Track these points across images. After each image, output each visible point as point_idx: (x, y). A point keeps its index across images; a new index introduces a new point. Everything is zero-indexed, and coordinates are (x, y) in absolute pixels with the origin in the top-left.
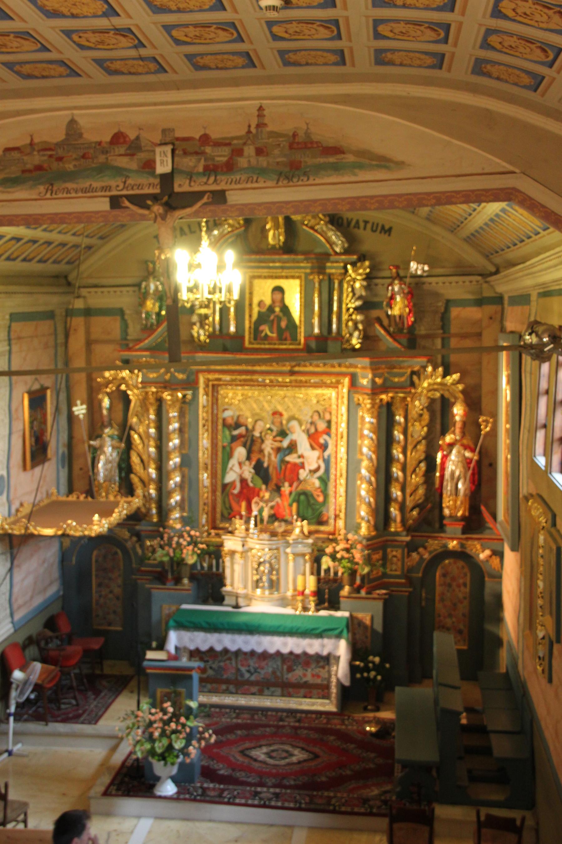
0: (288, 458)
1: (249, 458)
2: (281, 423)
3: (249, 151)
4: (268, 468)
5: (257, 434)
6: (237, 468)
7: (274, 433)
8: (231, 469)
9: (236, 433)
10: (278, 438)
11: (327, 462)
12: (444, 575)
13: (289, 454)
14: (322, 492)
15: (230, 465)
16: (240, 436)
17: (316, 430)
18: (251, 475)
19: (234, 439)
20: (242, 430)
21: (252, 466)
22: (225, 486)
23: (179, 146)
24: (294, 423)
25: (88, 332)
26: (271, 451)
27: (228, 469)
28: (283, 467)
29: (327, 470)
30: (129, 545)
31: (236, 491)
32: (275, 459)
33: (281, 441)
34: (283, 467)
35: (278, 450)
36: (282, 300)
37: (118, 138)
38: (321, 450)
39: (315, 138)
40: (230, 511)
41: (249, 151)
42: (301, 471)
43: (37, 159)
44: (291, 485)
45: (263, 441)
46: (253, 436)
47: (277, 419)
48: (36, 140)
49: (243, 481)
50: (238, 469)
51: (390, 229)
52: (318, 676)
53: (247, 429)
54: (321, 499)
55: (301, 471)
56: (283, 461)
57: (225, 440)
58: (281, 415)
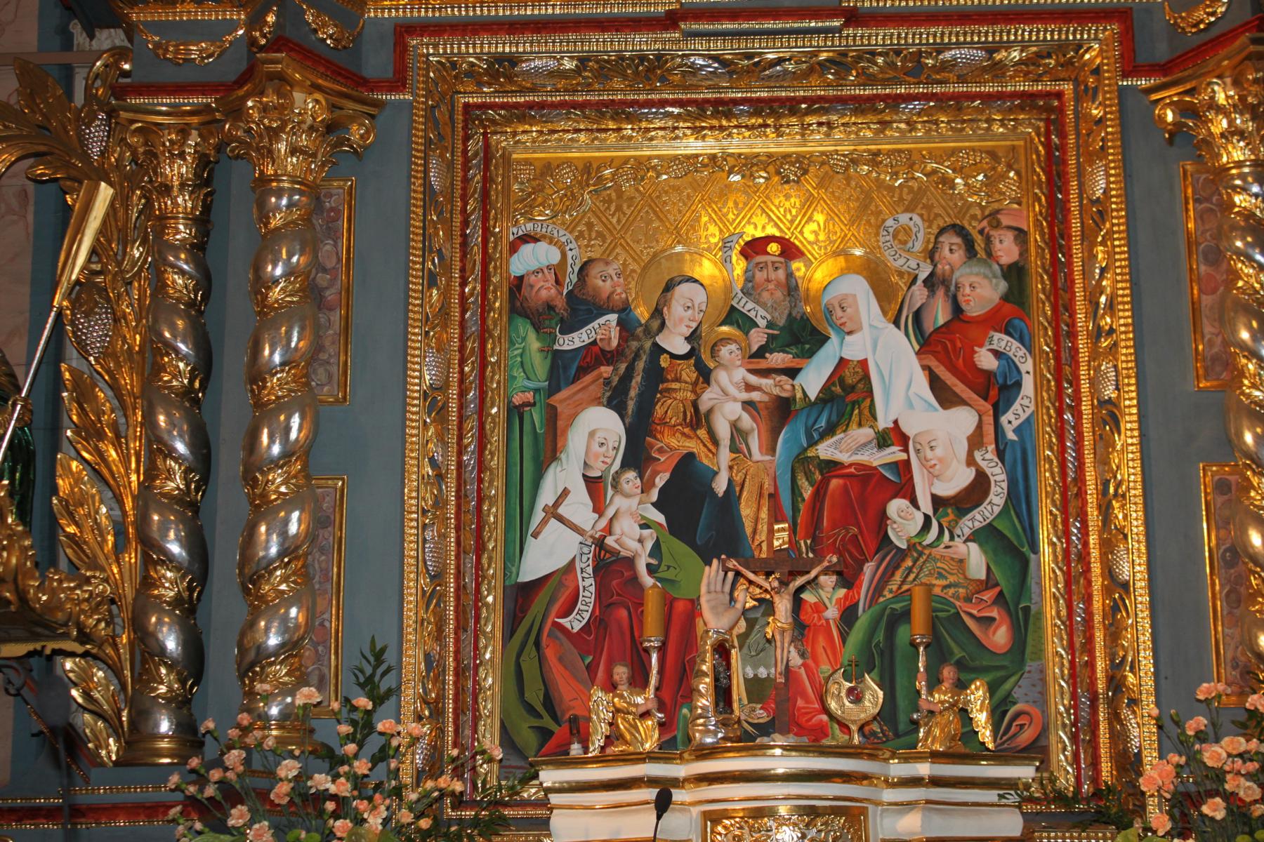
1: (637, 455)
4: (732, 497)
5: (676, 343)
6: (579, 508)
7: (757, 338)
8: (553, 513)
10: (777, 359)
13: (830, 430)
14: (1000, 599)
15: (546, 496)
16: (594, 356)
17: (957, 310)
18: (650, 535)
19: (564, 369)
20: (605, 328)
21: (654, 495)
22: (522, 596)
26: (747, 422)
27: (539, 515)
28: (807, 492)
29: (1021, 500)
31: (574, 623)
32: (766, 461)
33: (792, 373)
34: (807, 492)
35: (782, 411)
38: (987, 407)
40: (547, 722)
42: (896, 506)
45: (705, 375)
46: (658, 350)
49: (610, 566)
54: (1000, 637)
55: (896, 506)
56: (801, 462)
57: (521, 380)
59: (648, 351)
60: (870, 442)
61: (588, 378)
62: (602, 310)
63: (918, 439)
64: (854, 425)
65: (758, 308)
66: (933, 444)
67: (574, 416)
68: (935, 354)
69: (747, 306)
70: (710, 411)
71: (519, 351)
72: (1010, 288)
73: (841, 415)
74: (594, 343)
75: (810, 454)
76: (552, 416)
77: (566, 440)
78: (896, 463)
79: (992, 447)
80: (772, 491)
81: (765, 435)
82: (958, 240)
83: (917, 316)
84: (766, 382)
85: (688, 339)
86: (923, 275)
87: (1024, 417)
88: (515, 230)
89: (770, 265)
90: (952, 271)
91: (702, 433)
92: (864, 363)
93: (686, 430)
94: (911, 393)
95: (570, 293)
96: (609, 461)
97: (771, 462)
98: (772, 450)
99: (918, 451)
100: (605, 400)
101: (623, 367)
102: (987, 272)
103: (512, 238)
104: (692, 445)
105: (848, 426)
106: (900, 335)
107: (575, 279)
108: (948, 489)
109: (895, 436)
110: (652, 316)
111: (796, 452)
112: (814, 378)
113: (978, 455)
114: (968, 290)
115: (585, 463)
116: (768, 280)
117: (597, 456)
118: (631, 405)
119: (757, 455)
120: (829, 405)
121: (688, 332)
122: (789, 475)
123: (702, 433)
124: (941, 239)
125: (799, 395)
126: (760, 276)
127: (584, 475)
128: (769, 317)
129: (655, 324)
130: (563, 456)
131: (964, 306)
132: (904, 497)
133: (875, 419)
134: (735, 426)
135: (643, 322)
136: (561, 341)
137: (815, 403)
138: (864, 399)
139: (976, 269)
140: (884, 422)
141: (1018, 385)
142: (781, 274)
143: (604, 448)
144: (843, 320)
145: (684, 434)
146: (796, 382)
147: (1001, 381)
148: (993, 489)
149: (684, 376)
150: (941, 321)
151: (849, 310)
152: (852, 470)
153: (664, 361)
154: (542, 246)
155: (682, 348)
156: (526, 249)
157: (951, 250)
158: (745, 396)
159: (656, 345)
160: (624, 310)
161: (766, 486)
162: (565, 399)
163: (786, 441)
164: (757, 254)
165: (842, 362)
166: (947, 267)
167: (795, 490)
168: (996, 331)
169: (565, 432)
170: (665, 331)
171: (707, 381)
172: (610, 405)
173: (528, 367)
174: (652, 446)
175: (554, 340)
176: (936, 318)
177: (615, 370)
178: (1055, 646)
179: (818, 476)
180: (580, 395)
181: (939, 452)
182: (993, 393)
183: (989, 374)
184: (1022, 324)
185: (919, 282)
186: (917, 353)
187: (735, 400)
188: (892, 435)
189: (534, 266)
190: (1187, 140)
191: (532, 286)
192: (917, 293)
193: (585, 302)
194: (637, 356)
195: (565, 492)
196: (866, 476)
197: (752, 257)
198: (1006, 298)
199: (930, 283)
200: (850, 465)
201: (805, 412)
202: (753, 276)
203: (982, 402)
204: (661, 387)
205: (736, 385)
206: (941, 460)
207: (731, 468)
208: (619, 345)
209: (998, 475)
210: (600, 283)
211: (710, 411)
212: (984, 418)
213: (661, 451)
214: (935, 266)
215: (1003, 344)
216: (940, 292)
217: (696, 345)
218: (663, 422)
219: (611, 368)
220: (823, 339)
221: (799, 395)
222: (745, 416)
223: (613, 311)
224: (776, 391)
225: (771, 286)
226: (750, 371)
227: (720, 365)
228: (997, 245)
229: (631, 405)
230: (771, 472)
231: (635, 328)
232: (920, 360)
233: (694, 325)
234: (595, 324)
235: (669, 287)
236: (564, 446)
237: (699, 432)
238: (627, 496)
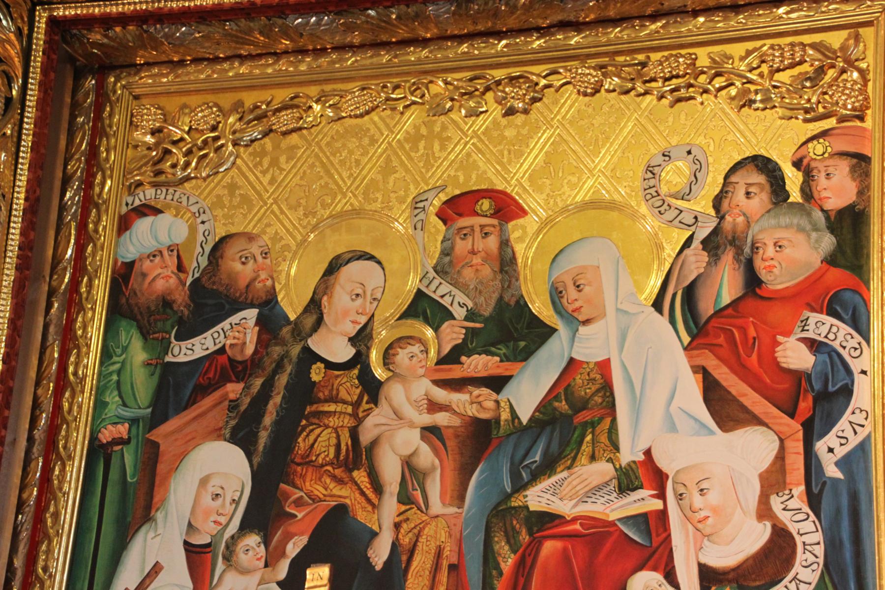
0: (538, 498)
1: (263, 513)
2: (506, 263)
5: (334, 346)
7: (453, 334)
9: (199, 347)
10: (478, 364)
13: (547, 467)
17: (753, 281)
19: (177, 389)
20: (240, 330)
26: (426, 457)
28: (508, 562)
33: (497, 383)
34: (508, 562)
35: (479, 438)
38: (794, 427)
45: (372, 389)
46: (310, 357)
53: (270, 320)
56: (501, 515)
58: (506, 208)
59: (295, 359)
60: (607, 483)
61: (207, 402)
62: (237, 306)
63: (682, 478)
64: (583, 459)
65: (455, 291)
66: (704, 485)
67: (182, 456)
68: (712, 348)
69: (442, 291)
70: (375, 443)
71: (117, 366)
72: (840, 247)
73: (564, 443)
74: (222, 350)
75: (515, 503)
76: (151, 457)
77: (167, 490)
78: (645, 516)
79: (799, 490)
80: (454, 560)
81: (451, 475)
82: (761, 179)
83: (690, 294)
84: (459, 399)
85: (353, 340)
86: (703, 233)
87: (854, 442)
88: (130, 200)
89: (477, 229)
90: (748, 224)
91: (361, 476)
92: (604, 366)
93: (338, 472)
94: (673, 408)
95: (196, 282)
96: (223, 520)
97: (456, 516)
98: (460, 498)
99: (680, 497)
100: (227, 432)
101: (258, 383)
102: (804, 222)
103: (124, 210)
104: (345, 494)
105: (574, 459)
106: (663, 321)
107: (204, 262)
109: (649, 474)
110: (306, 310)
111: (494, 500)
112: (527, 393)
113: (776, 503)
114: (770, 251)
115: (190, 525)
116: (473, 252)
117: (207, 513)
118: (263, 437)
119: (436, 506)
120: (548, 429)
121: (353, 330)
122: (481, 536)
123: (361, 476)
124: (733, 179)
125: (505, 415)
126: (462, 247)
127: (186, 543)
128: (470, 305)
129: (310, 321)
130: (159, 516)
131: (763, 275)
132: (655, 569)
133: (617, 448)
134: (409, 466)
135: (292, 317)
136: (176, 351)
137: (528, 427)
138: (601, 419)
139: (785, 220)
140: (629, 453)
141: (847, 392)
142: (492, 243)
143: (220, 501)
144: (577, 305)
145: (334, 478)
146: (502, 397)
147: (817, 386)
148: (800, 556)
149: (343, 394)
150: (726, 299)
151: (587, 289)
152: (577, 527)
153: (317, 373)
154: (165, 219)
155: (343, 352)
156: (143, 225)
157: (748, 193)
158: (427, 419)
159: (307, 350)
160: (268, 305)
161: (446, 553)
162: (173, 433)
163: (480, 485)
164: (461, 215)
165: (572, 364)
166: (741, 219)
167: (489, 558)
168: (813, 310)
169: (167, 478)
170: (322, 330)
171: (374, 400)
172: (234, 439)
173: (126, 388)
174: (287, 496)
175: (166, 349)
176: (718, 295)
177: (247, 387)
179: (524, 537)
180: (194, 426)
181: (713, 497)
182: (805, 405)
183: (798, 377)
184: (857, 297)
185: (696, 243)
186: (685, 349)
187: (412, 425)
188: (640, 472)
189: (151, 245)
191: (144, 275)
192: (692, 259)
193: (215, 294)
194: (279, 366)
195: (156, 569)
196: (597, 535)
197: (453, 220)
198: (831, 260)
199: (713, 244)
200: (574, 520)
201: (512, 440)
202: (452, 248)
203: (786, 419)
204: (308, 409)
205: (415, 404)
206: (715, 510)
207: (397, 526)
208: (256, 352)
209: (809, 534)
210: (238, 266)
211: (375, 443)
212: (789, 444)
213: (299, 503)
214: (722, 218)
215: (824, 330)
216: (728, 257)
217: (363, 348)
218: (307, 462)
219: (241, 386)
220: (545, 332)
221: (505, 415)
222: (425, 448)
223: (252, 306)
224: (473, 411)
225: (477, 260)
226: (438, 383)
227: (395, 376)
228: (821, 181)
229: (263, 437)
230: (456, 531)
231: (281, 329)
232: (690, 358)
233: (363, 320)
234: (225, 324)
235: (333, 268)
236: (163, 500)
237: (355, 474)
238: (244, 572)
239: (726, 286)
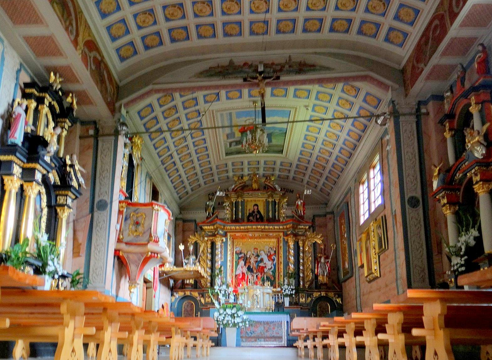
1: (245, 264)
3: (287, 66)
5: (248, 256)
10: (256, 258)
11: (275, 266)
12: (320, 308)
16: (242, 257)
19: (239, 258)
23: (266, 66)
24: (262, 252)
25: (183, 226)
30: (198, 299)
35: (256, 262)
36: (258, 208)
37: (245, 64)
39: (306, 63)
41: (287, 66)
42: (265, 269)
43: (220, 69)
44: (261, 274)
47: (256, 251)
48: (220, 65)
49: (243, 274)
50: (242, 268)
51: (293, 191)
52: (278, 333)
54: (273, 279)
56: (258, 265)
58: (257, 249)
108: (269, 268)
112: (259, 259)
178: (277, 280)
190: (287, 242)
239: (269, 254)
